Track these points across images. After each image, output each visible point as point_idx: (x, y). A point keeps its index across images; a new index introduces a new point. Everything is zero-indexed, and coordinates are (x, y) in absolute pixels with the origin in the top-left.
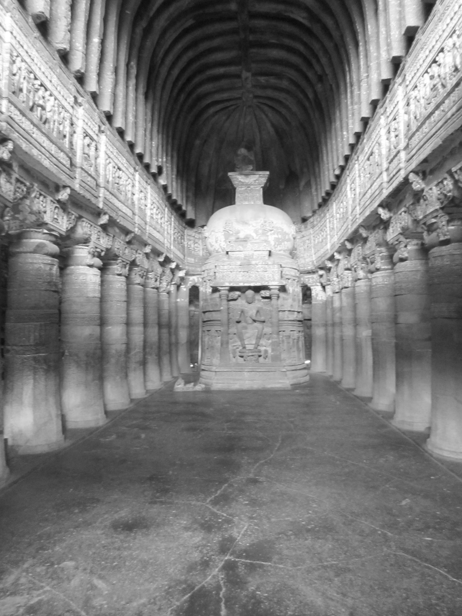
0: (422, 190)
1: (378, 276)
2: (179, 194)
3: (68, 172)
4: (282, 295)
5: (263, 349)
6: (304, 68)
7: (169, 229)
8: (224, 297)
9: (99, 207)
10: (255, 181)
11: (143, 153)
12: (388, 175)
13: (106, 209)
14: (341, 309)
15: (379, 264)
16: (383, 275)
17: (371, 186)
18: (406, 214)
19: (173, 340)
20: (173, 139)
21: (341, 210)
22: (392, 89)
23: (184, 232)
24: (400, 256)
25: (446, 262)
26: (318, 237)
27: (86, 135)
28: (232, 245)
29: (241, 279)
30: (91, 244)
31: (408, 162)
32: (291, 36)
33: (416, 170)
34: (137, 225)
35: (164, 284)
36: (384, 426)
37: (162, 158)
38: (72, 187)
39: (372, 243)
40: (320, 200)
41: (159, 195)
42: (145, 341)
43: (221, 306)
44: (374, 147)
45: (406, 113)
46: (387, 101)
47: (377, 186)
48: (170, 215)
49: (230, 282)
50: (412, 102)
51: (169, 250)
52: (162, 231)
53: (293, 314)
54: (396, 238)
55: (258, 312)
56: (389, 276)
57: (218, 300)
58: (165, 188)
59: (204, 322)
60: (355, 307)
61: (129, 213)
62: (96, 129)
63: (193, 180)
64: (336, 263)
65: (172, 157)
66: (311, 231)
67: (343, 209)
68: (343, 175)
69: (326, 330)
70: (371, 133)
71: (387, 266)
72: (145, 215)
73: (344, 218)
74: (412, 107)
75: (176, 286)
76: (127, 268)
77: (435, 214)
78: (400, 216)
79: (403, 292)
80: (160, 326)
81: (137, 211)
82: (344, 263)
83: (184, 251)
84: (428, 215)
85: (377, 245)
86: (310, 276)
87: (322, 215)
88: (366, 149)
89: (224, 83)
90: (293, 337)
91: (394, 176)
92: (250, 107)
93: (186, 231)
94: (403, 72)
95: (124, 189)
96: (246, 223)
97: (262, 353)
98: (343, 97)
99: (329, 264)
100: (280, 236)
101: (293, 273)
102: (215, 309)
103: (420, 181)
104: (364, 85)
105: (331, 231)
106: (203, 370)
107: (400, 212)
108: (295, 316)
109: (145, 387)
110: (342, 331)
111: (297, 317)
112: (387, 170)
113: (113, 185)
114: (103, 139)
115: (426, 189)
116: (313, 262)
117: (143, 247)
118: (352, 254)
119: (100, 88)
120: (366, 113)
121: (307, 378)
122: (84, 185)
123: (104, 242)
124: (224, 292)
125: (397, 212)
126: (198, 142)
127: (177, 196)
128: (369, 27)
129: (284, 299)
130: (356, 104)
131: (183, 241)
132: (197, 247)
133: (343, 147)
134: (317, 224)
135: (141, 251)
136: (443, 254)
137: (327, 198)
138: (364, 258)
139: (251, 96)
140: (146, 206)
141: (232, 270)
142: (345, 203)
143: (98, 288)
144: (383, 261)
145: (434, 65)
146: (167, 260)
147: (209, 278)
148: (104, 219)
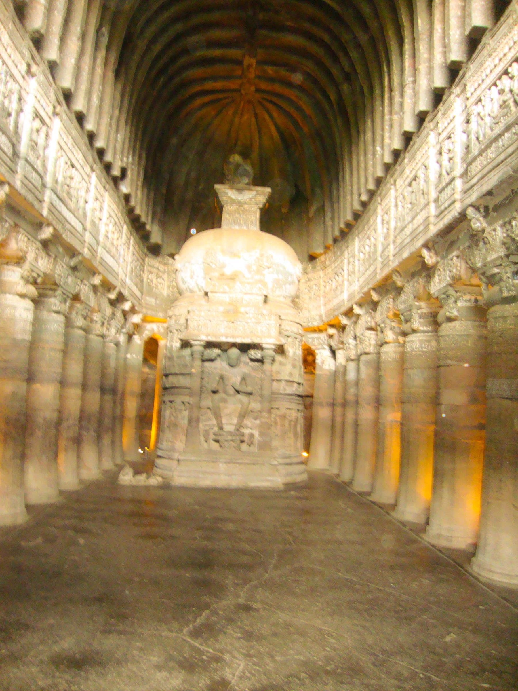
0: (483, 231)
1: (414, 339)
2: (144, 207)
3: (9, 163)
4: (279, 358)
5: (246, 431)
6: (328, 62)
7: (126, 254)
8: (197, 356)
9: (42, 215)
10: (251, 199)
11: (105, 147)
12: (438, 207)
13: (51, 218)
14: (357, 383)
15: (417, 323)
16: (421, 338)
17: (413, 219)
18: (459, 260)
19: (118, 411)
20: (144, 133)
21: (367, 248)
22: (446, 100)
23: (144, 261)
24: (448, 314)
25: (510, 324)
26: (330, 282)
27: (37, 115)
29: (223, 331)
30: (27, 266)
31: (465, 192)
32: (313, 20)
33: (477, 204)
34: (86, 245)
35: (113, 331)
36: (415, 542)
37: (128, 158)
38: (12, 184)
39: (408, 296)
40: (337, 233)
41: (118, 207)
42: (82, 410)
43: (192, 367)
44: (418, 170)
45: (464, 132)
46: (439, 115)
47: (421, 221)
48: (129, 236)
49: (208, 335)
50: (473, 119)
51: (123, 283)
52: (118, 256)
53: (292, 386)
54: (444, 291)
55: (244, 379)
56: (429, 341)
57: (188, 359)
58: (127, 198)
59: (165, 389)
60: (378, 382)
61: (79, 227)
62: (50, 110)
63: (164, 190)
64: (354, 319)
65: (140, 157)
66: (321, 274)
67: (370, 247)
68: (372, 203)
69: (333, 411)
70: (416, 152)
71: (426, 327)
72: (98, 231)
73: (371, 258)
74: (473, 126)
75: (127, 336)
76: (68, 303)
77: (498, 262)
78: (450, 262)
79: (449, 362)
80: (103, 390)
81: (88, 225)
82: (366, 320)
83: (142, 287)
84: (489, 263)
85: (415, 297)
86: (315, 335)
87: (338, 253)
88: (407, 171)
89: (219, 69)
90: (290, 419)
91: (446, 209)
92: (249, 102)
93: (147, 260)
94: (463, 81)
95: (75, 192)
97: (246, 438)
98: (378, 103)
99: (344, 321)
101: (296, 328)
102: (183, 372)
103: (481, 219)
104: (408, 92)
105: (349, 275)
106: (159, 457)
107: (450, 257)
108: (294, 389)
109: (78, 474)
110: (357, 414)
111: (296, 390)
112: (436, 200)
113: (62, 186)
114: (57, 124)
115: (488, 230)
116: (321, 316)
117: (91, 276)
118: (379, 308)
119: (60, 57)
120: (409, 126)
121: (304, 477)
122: (26, 182)
123: (44, 264)
124: (198, 348)
125: (447, 257)
126: (174, 141)
127: (141, 210)
128: (419, 21)
129: (281, 364)
130: (396, 113)
131: (142, 272)
132: (160, 284)
133: (374, 166)
134: (330, 265)
135: (88, 281)
136: (506, 314)
137: (346, 230)
138: (396, 315)
139: (253, 88)
140: (100, 220)
142: (372, 239)
143: (29, 327)
144: (421, 320)
145: (504, 77)
146: (121, 298)
147: (178, 327)
148: (47, 233)
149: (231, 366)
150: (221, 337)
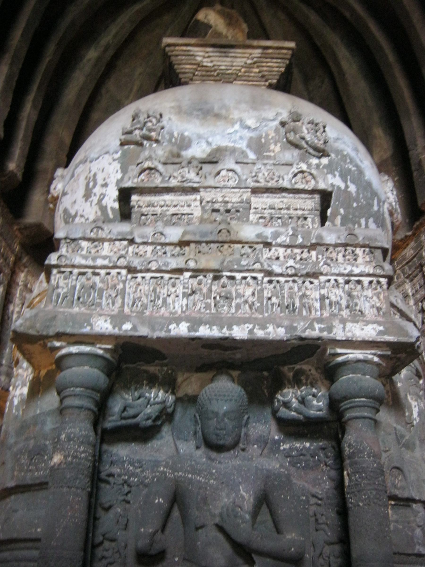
10: (249, 67)
23: (13, 273)
28: (147, 164)
29: (179, 305)
49: (119, 319)
96: (217, 116)
100: (352, 188)
102: (29, 479)
126: (92, 54)
141: (136, 263)
149: (215, 446)
150: (172, 327)
